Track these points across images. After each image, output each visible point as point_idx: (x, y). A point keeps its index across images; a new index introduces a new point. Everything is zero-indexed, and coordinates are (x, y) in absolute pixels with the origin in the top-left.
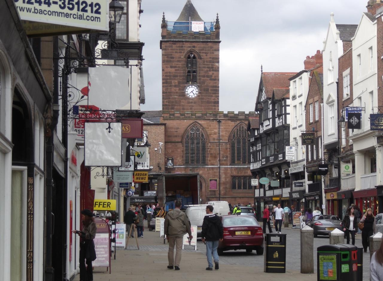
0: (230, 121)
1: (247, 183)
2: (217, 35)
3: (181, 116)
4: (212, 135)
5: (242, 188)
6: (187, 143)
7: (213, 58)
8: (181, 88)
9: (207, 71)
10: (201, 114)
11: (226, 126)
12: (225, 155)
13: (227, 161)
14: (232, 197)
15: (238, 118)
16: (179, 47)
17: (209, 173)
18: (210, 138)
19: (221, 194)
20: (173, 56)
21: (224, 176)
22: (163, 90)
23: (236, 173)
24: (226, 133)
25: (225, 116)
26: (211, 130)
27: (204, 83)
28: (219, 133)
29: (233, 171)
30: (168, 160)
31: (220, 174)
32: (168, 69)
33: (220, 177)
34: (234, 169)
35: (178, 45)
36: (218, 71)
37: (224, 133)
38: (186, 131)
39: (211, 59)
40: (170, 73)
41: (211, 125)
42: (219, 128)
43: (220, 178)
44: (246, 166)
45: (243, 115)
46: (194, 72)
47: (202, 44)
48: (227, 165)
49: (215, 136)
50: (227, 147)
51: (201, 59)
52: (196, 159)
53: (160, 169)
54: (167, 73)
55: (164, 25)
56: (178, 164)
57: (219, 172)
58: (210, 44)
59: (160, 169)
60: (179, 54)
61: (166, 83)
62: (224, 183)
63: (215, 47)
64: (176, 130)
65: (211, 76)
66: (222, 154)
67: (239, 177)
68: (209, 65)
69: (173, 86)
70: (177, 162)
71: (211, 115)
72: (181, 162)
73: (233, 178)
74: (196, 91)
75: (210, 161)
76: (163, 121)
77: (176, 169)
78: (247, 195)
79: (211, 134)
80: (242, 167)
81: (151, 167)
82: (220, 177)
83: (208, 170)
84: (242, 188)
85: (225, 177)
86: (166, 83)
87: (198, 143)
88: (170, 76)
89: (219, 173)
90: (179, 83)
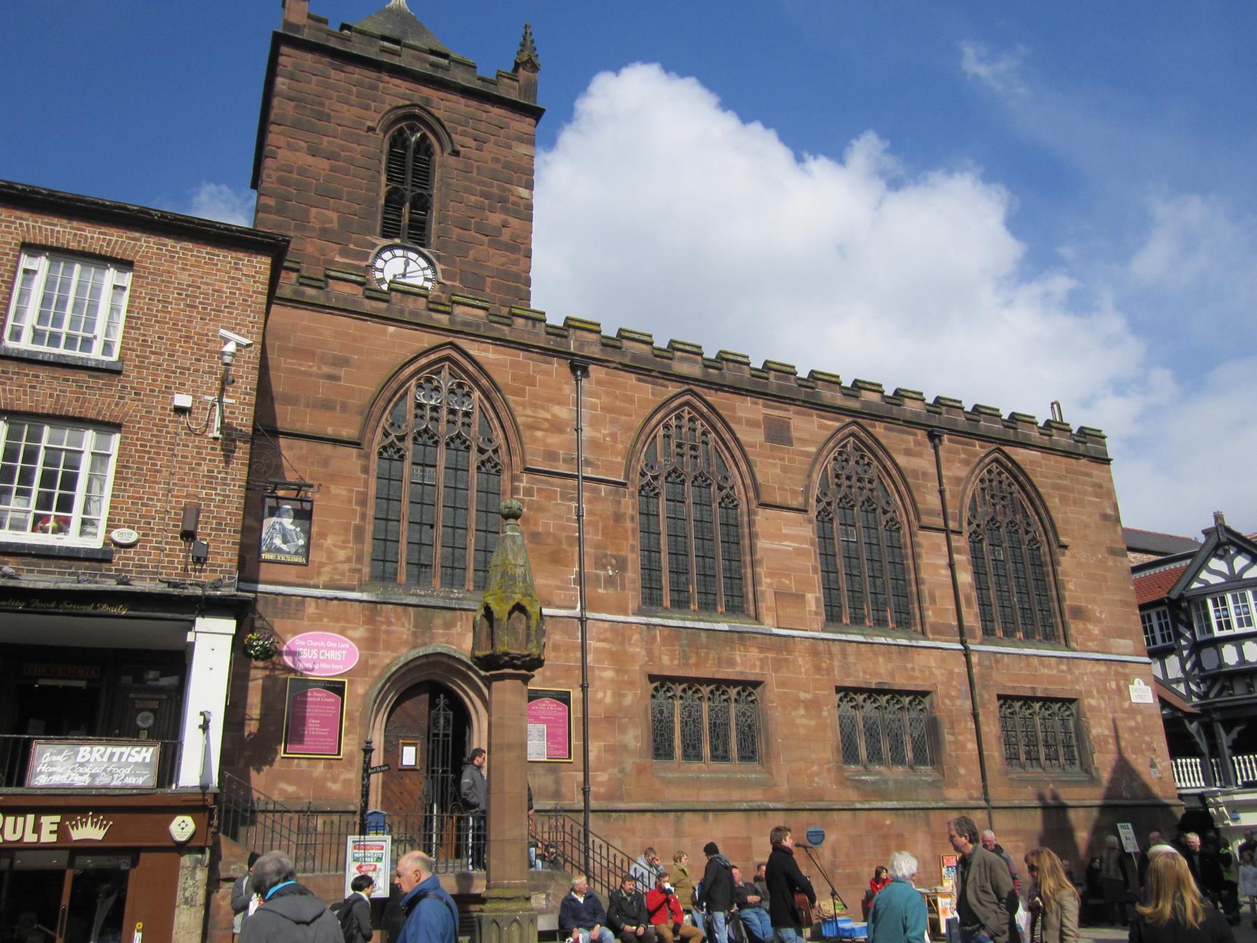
1: (727, 725)
2: (530, 88)
3: (367, 301)
4: (539, 434)
5: (706, 750)
6: (391, 453)
7: (507, 166)
8: (351, 246)
10: (481, 313)
11: (617, 397)
12: (609, 553)
13: (623, 587)
15: (670, 367)
16: (359, 84)
18: (529, 447)
20: (326, 110)
21: (609, 674)
23: (676, 662)
24: (613, 436)
25: (607, 343)
26: (535, 406)
31: (590, 658)
32: (298, 154)
33: (584, 677)
34: (664, 638)
35: (358, 73)
36: (529, 219)
37: (606, 432)
39: (499, 167)
40: (302, 171)
41: (534, 378)
43: (584, 688)
45: (695, 362)
47: (463, 100)
48: (625, 613)
50: (623, 510)
51: (456, 153)
52: (444, 557)
56: (324, 579)
60: (356, 111)
63: (522, 124)
64: (326, 369)
66: (598, 546)
67: (692, 683)
69: (313, 229)
70: (322, 565)
71: (534, 326)
72: (347, 566)
73: (656, 689)
74: (426, 279)
77: (311, 608)
78: (736, 795)
81: (116, 535)
82: (584, 677)
84: (706, 750)
85: (612, 681)
89: (579, 654)
90: (345, 225)
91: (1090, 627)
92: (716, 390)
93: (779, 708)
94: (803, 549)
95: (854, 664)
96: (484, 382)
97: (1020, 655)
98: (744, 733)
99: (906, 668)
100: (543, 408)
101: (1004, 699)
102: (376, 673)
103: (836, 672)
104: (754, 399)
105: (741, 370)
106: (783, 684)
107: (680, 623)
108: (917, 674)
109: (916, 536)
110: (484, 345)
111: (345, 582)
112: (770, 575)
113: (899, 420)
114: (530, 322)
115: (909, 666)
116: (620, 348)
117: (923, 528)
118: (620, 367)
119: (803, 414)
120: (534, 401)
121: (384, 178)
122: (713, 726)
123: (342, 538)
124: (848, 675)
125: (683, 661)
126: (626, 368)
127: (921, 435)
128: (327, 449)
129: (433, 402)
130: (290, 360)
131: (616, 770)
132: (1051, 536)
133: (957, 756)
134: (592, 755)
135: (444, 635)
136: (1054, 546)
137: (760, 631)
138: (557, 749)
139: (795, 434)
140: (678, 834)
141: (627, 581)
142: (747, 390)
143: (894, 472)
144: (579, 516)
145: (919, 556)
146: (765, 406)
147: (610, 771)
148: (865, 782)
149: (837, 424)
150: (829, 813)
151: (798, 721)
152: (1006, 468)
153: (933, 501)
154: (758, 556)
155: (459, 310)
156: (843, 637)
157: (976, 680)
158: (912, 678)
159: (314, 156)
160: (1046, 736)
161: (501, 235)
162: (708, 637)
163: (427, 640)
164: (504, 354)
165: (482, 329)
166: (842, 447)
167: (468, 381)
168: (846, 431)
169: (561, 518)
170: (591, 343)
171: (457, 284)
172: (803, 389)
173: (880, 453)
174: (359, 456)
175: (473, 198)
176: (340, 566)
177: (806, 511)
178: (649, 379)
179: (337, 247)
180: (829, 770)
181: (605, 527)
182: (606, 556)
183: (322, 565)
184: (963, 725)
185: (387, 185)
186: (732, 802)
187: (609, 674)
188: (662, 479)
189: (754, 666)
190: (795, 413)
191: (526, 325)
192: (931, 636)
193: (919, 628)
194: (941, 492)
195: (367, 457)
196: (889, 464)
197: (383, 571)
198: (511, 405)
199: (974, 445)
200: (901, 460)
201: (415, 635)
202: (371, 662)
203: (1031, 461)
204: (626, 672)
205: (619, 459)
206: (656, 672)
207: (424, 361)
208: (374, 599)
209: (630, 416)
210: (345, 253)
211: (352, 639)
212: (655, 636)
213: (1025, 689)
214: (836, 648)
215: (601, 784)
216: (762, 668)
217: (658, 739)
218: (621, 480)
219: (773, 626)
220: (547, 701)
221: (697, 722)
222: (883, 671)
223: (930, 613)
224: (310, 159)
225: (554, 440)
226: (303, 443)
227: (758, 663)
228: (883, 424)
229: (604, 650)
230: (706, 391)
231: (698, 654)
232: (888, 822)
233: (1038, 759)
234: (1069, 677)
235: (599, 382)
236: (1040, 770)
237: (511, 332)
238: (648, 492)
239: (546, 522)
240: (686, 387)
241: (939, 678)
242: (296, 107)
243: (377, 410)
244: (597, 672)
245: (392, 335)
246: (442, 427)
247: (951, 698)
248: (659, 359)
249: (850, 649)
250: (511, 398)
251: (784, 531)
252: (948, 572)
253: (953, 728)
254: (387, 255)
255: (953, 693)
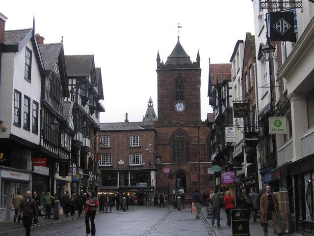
6: (174, 145)
9: (191, 91)
28: (199, 137)
30: (157, 157)
38: (173, 136)
42: (199, 133)
46: (182, 92)
49: (196, 139)
53: (150, 165)
55: (158, 60)
58: (193, 71)
59: (150, 165)
87: (183, 145)
197: (174, 160)
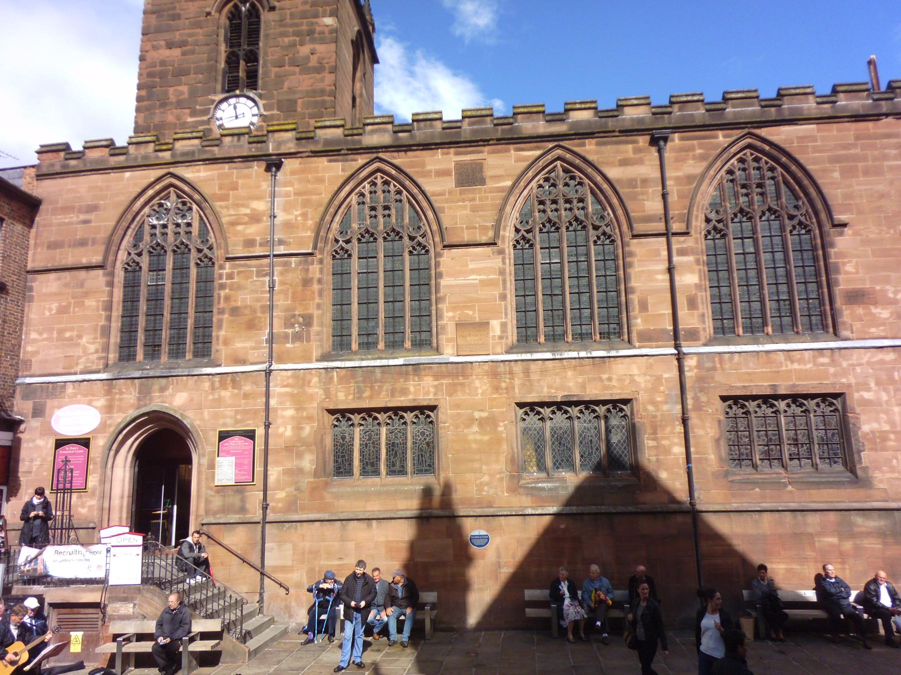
0: (325, 159)
4: (240, 228)
8: (198, 107)
9: (293, 45)
10: (197, 142)
11: (308, 181)
13: (308, 340)
14: (326, 516)
15: (360, 142)
17: (219, 402)
18: (232, 240)
19: (272, 504)
20: (178, 11)
21: (290, 412)
22: (136, 122)
23: (351, 397)
24: (304, 215)
26: (237, 206)
27: (280, 78)
29: (332, 389)
31: (273, 402)
32: (160, 51)
34: (341, 379)
39: (307, 7)
40: (163, 63)
41: (237, 183)
43: (267, 426)
44: (400, 361)
45: (385, 131)
48: (309, 361)
50: (310, 276)
51: (272, 9)
54: (153, 65)
57: (267, 395)
61: (149, 97)
62: (289, 448)
64: (82, 217)
65: (307, 59)
67: (369, 412)
68: (302, 24)
69: (171, 103)
70: (79, 357)
71: (239, 140)
72: (95, 356)
74: (253, 115)
75: (226, 343)
76: (35, 182)
77: (70, 389)
79: (234, 224)
80: (378, 363)
83: (213, 388)
85: (293, 418)
86: (149, 97)
88: (162, 75)
90: (193, 94)
91: (874, 310)
92: (406, 151)
93: (451, 428)
94: (491, 280)
95: (539, 380)
96: (197, 197)
97: (758, 352)
98: (422, 450)
99: (601, 379)
100: (243, 206)
101: (733, 400)
102: (112, 429)
103: (517, 390)
104: (445, 150)
105: (432, 126)
106: (457, 406)
107: (356, 364)
108: (614, 383)
109: (628, 245)
110: (197, 167)
111: (94, 368)
112: (453, 309)
113: (614, 131)
114: (236, 138)
115: (605, 376)
116: (312, 138)
117: (635, 236)
118: (311, 154)
119: (499, 152)
120: (237, 202)
121: (223, 48)
122: (391, 446)
123: (92, 336)
124: (530, 392)
125: (358, 395)
126: (316, 154)
127: (643, 141)
128: (83, 274)
129: (162, 222)
130: (59, 217)
131: (293, 489)
132: (823, 216)
133: (658, 461)
134: (272, 479)
135: (159, 397)
136: (827, 227)
137: (437, 361)
138: (243, 475)
139: (488, 173)
140: (343, 539)
141: (312, 334)
142: (436, 144)
143: (605, 186)
144: (272, 288)
145: (631, 265)
146: (456, 154)
147: (287, 489)
148: (543, 489)
149: (538, 153)
150: (497, 518)
151: (471, 437)
152: (762, 152)
153: (654, 206)
154: (441, 294)
155: (179, 145)
156: (528, 356)
157: (688, 384)
158: (606, 388)
159: (170, 48)
160: (796, 434)
161: (309, 62)
162: (383, 373)
163: (148, 402)
164: (210, 170)
165: (196, 154)
166: (549, 172)
167: (187, 199)
168: (549, 157)
169: (257, 292)
170: (285, 142)
171: (275, 112)
172: (500, 128)
173: (589, 170)
174: (104, 275)
175: (286, 40)
176: (91, 357)
177: (495, 244)
178: (340, 158)
179: (187, 111)
180: (502, 479)
181: (294, 293)
182: (294, 316)
183: (79, 357)
184: (668, 429)
185: (226, 52)
186: (398, 510)
187: (290, 412)
188: (355, 241)
189: (428, 393)
190: (489, 153)
191: (232, 141)
192: (637, 344)
193: (626, 337)
194: (664, 196)
195: (112, 274)
196: (599, 179)
198: (218, 209)
199: (716, 137)
200: (613, 173)
201: (139, 399)
202: (108, 422)
203: (798, 138)
204: (305, 409)
205: (309, 233)
206: (331, 407)
207: (150, 192)
208: (110, 377)
209: (320, 194)
210: (194, 113)
211: (96, 407)
212: (332, 378)
213: (762, 387)
214: (517, 368)
215: (279, 500)
216: (435, 394)
217: (340, 460)
218: (310, 251)
219: (452, 355)
220: (236, 438)
221: (377, 444)
222: (571, 384)
223: (639, 321)
224: (167, 52)
225: (252, 230)
226: (67, 274)
227: (432, 390)
228: (594, 141)
229: (286, 394)
230: (395, 154)
231: (372, 388)
232: (563, 526)
233: (780, 459)
234: (832, 370)
235: (293, 173)
236: (782, 471)
237: (219, 150)
238: (341, 255)
239: (244, 298)
240: (375, 155)
241: (643, 385)
242: (157, 17)
243: (116, 238)
244: (279, 412)
245: (129, 179)
246: (171, 237)
247: (653, 402)
248: (349, 138)
249: (533, 367)
250: (217, 205)
251: (471, 266)
252: (667, 277)
253: (655, 433)
254: (224, 106)
255: (659, 399)
